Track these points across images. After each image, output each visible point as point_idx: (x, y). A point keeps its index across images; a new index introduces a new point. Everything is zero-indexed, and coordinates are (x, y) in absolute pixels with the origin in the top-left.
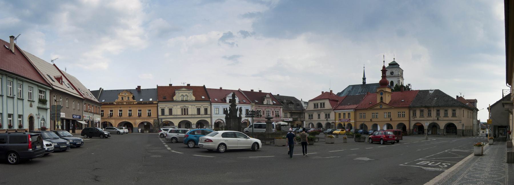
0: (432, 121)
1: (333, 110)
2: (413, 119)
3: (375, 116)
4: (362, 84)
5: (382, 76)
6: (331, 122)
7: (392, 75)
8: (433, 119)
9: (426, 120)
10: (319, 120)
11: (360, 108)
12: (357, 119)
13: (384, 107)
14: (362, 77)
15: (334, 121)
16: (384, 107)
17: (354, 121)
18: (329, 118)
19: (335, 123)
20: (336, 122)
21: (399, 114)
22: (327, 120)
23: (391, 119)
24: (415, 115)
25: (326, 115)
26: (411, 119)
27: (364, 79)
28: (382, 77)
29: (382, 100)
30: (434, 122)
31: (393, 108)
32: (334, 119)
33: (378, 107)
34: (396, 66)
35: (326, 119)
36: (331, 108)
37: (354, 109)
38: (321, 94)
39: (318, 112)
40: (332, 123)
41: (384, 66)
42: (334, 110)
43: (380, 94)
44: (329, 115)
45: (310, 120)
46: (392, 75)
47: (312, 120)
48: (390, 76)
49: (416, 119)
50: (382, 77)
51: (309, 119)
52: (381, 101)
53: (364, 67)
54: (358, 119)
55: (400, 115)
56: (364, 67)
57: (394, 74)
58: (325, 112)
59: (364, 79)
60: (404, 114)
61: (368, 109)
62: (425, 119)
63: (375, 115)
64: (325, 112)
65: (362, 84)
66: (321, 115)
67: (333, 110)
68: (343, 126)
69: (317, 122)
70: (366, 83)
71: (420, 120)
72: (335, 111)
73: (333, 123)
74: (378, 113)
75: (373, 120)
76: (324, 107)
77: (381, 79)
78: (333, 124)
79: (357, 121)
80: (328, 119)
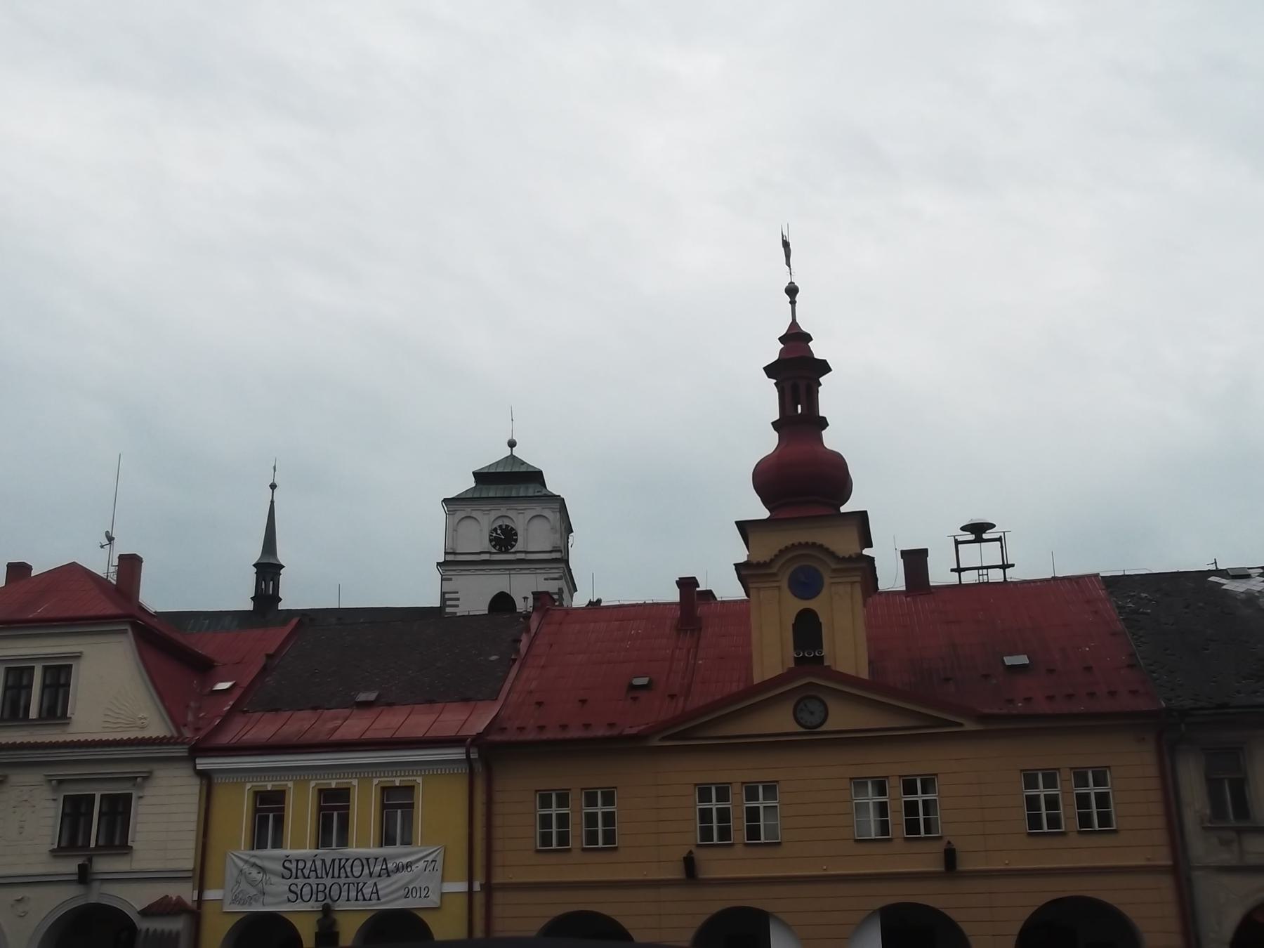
1: (181, 751)
2: (1226, 857)
3: (739, 826)
4: (249, 606)
5: (776, 416)
6: (134, 899)
7: (500, 552)
11: (521, 729)
12: (498, 858)
13: (841, 718)
14: (256, 553)
15: (187, 893)
16: (841, 718)
17: (462, 887)
18: (117, 841)
19: (195, 914)
21: (1042, 792)
22: (84, 876)
23: (950, 856)
24: (1242, 808)
25: (75, 811)
26: (1201, 848)
27: (268, 570)
28: (776, 425)
29: (819, 645)
31: (969, 726)
32: (186, 860)
33: (781, 721)
34: (531, 490)
35: (70, 866)
36: (157, 727)
37: (478, 740)
40: (146, 913)
42: (198, 750)
43: (784, 584)
44: (119, 809)
46: (507, 552)
48: (486, 557)
50: (776, 425)
52: (797, 660)
56: (273, 486)
57: (519, 546)
59: (268, 570)
60: (1103, 800)
61: (655, 742)
63: (738, 804)
65: (249, 606)
67: (181, 751)
70: (281, 606)
72: (203, 764)
74: (770, 790)
75: (714, 865)
76: (56, 711)
77: (769, 442)
78: (177, 925)
79: (499, 878)
80: (103, 865)
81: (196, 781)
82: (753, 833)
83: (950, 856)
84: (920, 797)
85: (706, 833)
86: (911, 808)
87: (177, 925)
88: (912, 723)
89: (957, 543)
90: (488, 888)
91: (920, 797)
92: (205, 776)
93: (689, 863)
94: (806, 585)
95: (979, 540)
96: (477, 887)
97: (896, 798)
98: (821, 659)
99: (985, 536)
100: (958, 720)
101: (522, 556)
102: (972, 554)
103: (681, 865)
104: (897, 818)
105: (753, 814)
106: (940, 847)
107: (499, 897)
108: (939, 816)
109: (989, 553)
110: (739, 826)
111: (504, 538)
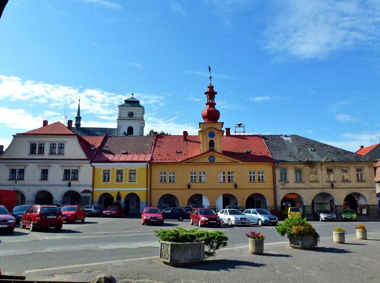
0: (321, 190)
2: (282, 187)
3: (198, 180)
6: (79, 190)
8: (321, 186)
9: (309, 187)
10: (44, 182)
12: (152, 184)
15: (91, 189)
17: (145, 189)
18: (76, 179)
19: (92, 192)
20: (95, 189)
21: (252, 175)
22: (69, 185)
23: (236, 186)
24: (286, 179)
26: (278, 184)
30: (325, 192)
32: (90, 182)
35: (67, 182)
37: (149, 162)
38: (41, 125)
39: (42, 164)
41: (211, 84)
43: (208, 135)
44: (76, 172)
45: (13, 182)
47: (19, 182)
49: (287, 185)
51: (10, 179)
52: (210, 149)
53: (79, 100)
54: (156, 184)
55: (254, 176)
56: (79, 100)
58: (64, 165)
60: (262, 177)
62: (306, 187)
64: (64, 165)
66: (50, 173)
67: (89, 161)
68: (115, 200)
69: (35, 190)
70: (81, 126)
71: (295, 188)
72: (93, 164)
73: (86, 191)
75: (193, 185)
78: (89, 195)
79: (152, 187)
80: (73, 183)
81: (92, 168)
82: (200, 181)
83: (236, 186)
84: (231, 175)
85: (192, 180)
86: (229, 177)
87: (89, 195)
88: (231, 162)
89: (236, 127)
90: (150, 189)
91: (231, 175)
92: (92, 166)
93: (189, 186)
94: (212, 135)
95: (240, 127)
96: (148, 189)
97: (227, 175)
98: (214, 149)
99: (241, 126)
100: (239, 162)
101: (135, 119)
102: (238, 129)
103: (187, 186)
104: (227, 179)
105: (201, 177)
106: (234, 184)
107: (152, 191)
108: (234, 179)
109: (241, 129)
110: (198, 180)
111: (131, 115)
